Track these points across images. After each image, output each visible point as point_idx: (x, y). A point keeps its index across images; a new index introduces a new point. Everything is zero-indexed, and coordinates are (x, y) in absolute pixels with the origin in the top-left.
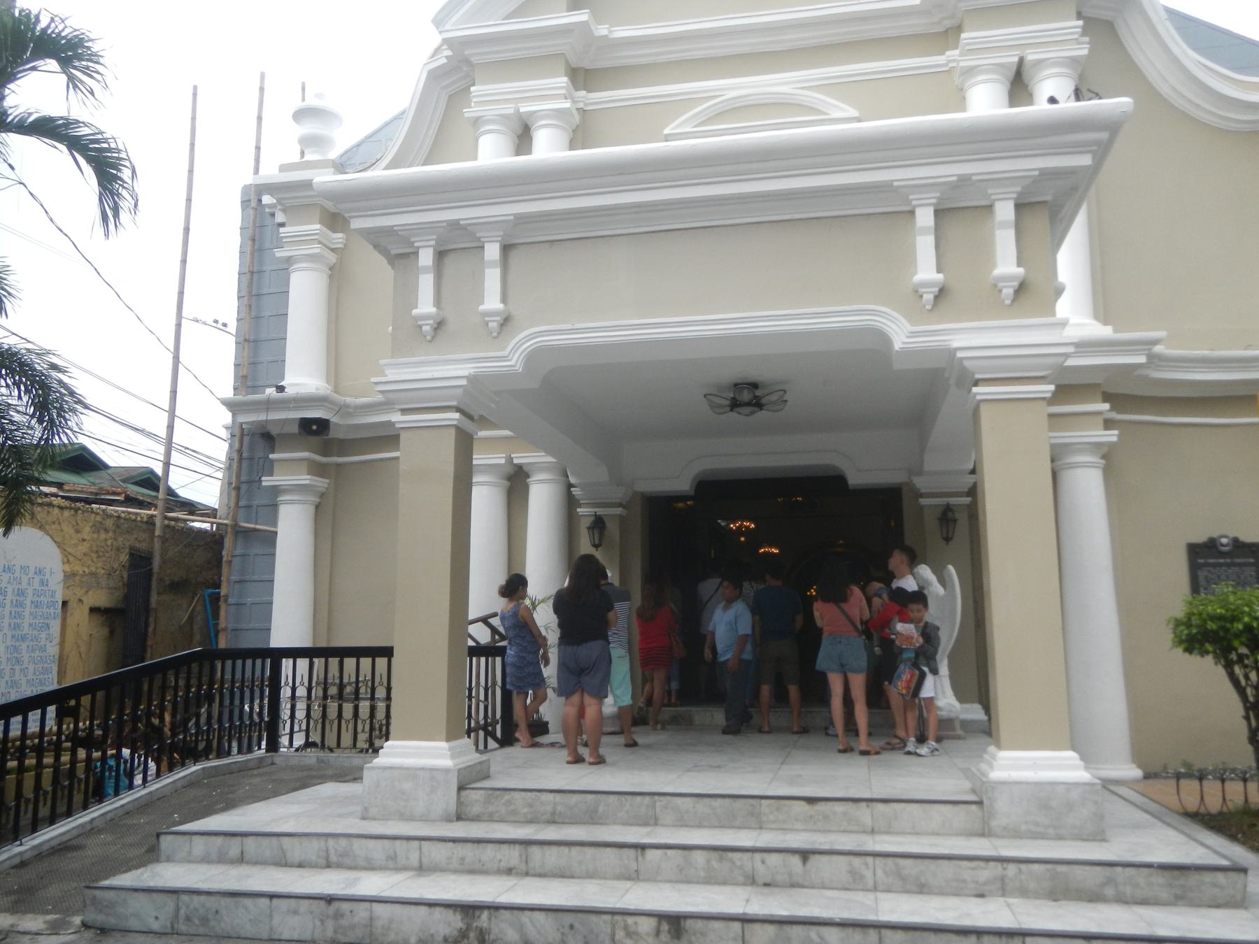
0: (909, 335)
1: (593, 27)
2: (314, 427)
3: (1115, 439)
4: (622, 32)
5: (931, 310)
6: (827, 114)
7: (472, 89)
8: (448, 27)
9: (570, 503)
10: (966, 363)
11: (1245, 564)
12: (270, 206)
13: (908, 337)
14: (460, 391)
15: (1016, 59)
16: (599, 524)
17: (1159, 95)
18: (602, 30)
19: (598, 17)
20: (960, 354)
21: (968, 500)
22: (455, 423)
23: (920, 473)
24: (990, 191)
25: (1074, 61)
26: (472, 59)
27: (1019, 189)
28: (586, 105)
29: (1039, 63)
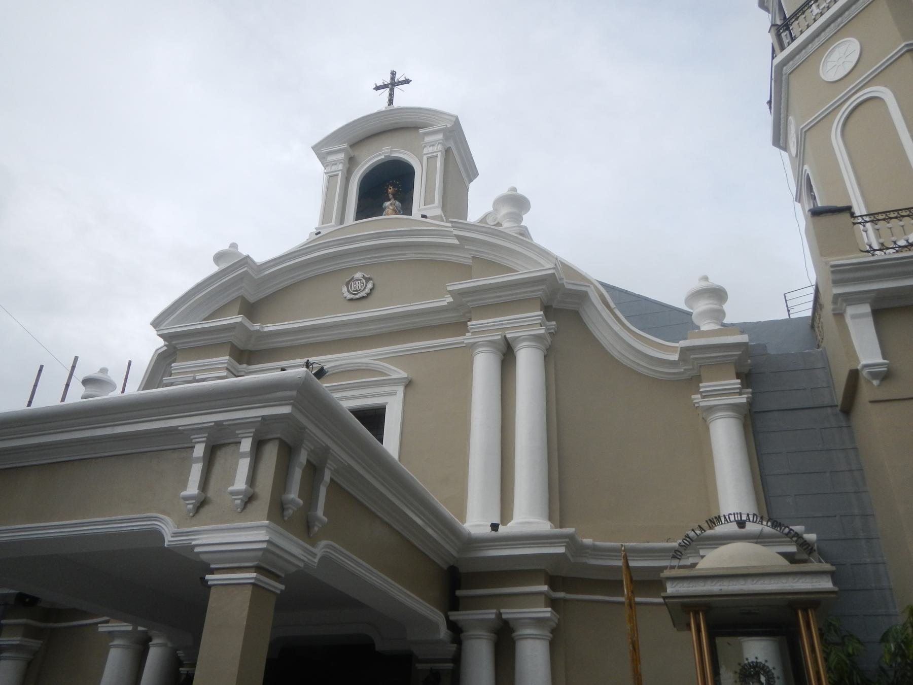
0: (173, 535)
4: (269, 327)
5: (194, 516)
6: (391, 376)
8: (162, 328)
13: (172, 537)
17: (612, 357)
20: (197, 550)
21: (449, 666)
24: (237, 432)
25: (537, 338)
26: (177, 346)
29: (516, 338)
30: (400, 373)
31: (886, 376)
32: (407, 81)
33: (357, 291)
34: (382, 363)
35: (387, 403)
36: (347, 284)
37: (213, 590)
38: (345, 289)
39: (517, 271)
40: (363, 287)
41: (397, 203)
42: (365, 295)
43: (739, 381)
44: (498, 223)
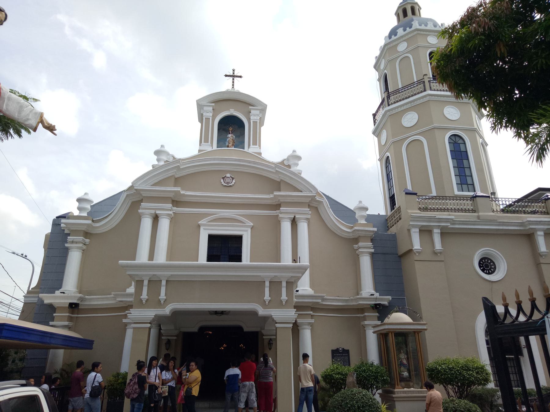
1: (181, 191)
2: (74, 306)
3: (313, 322)
7: (142, 204)
9: (160, 335)
10: (275, 319)
11: (347, 356)
12: (63, 227)
14: (152, 318)
15: (293, 217)
16: (169, 342)
18: (182, 192)
19: (183, 189)
20: (273, 317)
22: (149, 327)
23: (264, 329)
27: (287, 279)
28: (175, 211)
30: (250, 224)
31: (419, 253)
32: (240, 77)
33: (228, 182)
34: (240, 217)
35: (243, 234)
36: (223, 178)
37: (277, 328)
38: (222, 181)
39: (302, 192)
40: (231, 182)
41: (234, 137)
42: (232, 185)
43: (372, 244)
44: (289, 165)
